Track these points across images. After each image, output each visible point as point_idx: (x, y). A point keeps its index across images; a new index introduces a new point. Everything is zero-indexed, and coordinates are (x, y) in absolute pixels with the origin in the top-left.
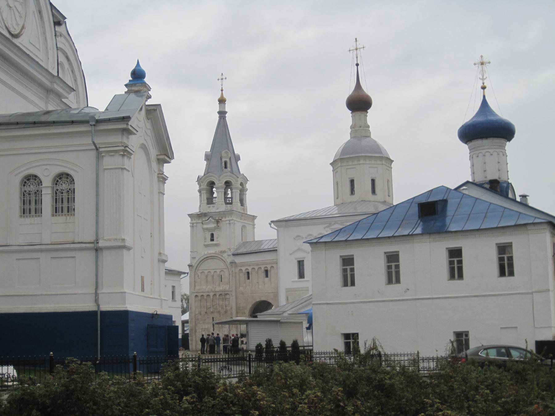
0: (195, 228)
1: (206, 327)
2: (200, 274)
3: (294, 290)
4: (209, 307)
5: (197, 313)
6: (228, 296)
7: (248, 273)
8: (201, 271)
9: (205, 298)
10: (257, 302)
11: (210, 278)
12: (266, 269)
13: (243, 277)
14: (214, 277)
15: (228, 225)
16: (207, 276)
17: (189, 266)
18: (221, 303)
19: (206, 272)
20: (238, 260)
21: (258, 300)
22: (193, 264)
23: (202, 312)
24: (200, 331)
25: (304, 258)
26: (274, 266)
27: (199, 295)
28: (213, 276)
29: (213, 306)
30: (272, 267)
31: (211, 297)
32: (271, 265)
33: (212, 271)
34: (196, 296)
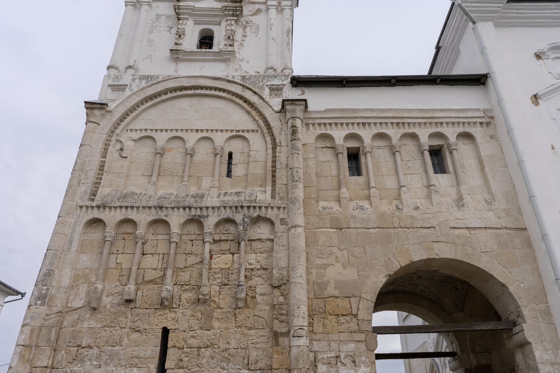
0: (145, 7)
2: (129, 144)
4: (150, 275)
5: (78, 303)
6: (263, 231)
8: (136, 136)
9: (141, 231)
10: (412, 263)
11: (175, 157)
12: (436, 142)
13: (334, 166)
14: (197, 158)
15: (273, 11)
16: (160, 153)
17: (90, 106)
18: (222, 261)
20: (319, 101)
22: (111, 106)
23: (106, 300)
26: (476, 131)
27: (111, 217)
28: (190, 154)
29: (177, 270)
30: (467, 136)
31: (175, 228)
32: (460, 129)
34: (96, 222)
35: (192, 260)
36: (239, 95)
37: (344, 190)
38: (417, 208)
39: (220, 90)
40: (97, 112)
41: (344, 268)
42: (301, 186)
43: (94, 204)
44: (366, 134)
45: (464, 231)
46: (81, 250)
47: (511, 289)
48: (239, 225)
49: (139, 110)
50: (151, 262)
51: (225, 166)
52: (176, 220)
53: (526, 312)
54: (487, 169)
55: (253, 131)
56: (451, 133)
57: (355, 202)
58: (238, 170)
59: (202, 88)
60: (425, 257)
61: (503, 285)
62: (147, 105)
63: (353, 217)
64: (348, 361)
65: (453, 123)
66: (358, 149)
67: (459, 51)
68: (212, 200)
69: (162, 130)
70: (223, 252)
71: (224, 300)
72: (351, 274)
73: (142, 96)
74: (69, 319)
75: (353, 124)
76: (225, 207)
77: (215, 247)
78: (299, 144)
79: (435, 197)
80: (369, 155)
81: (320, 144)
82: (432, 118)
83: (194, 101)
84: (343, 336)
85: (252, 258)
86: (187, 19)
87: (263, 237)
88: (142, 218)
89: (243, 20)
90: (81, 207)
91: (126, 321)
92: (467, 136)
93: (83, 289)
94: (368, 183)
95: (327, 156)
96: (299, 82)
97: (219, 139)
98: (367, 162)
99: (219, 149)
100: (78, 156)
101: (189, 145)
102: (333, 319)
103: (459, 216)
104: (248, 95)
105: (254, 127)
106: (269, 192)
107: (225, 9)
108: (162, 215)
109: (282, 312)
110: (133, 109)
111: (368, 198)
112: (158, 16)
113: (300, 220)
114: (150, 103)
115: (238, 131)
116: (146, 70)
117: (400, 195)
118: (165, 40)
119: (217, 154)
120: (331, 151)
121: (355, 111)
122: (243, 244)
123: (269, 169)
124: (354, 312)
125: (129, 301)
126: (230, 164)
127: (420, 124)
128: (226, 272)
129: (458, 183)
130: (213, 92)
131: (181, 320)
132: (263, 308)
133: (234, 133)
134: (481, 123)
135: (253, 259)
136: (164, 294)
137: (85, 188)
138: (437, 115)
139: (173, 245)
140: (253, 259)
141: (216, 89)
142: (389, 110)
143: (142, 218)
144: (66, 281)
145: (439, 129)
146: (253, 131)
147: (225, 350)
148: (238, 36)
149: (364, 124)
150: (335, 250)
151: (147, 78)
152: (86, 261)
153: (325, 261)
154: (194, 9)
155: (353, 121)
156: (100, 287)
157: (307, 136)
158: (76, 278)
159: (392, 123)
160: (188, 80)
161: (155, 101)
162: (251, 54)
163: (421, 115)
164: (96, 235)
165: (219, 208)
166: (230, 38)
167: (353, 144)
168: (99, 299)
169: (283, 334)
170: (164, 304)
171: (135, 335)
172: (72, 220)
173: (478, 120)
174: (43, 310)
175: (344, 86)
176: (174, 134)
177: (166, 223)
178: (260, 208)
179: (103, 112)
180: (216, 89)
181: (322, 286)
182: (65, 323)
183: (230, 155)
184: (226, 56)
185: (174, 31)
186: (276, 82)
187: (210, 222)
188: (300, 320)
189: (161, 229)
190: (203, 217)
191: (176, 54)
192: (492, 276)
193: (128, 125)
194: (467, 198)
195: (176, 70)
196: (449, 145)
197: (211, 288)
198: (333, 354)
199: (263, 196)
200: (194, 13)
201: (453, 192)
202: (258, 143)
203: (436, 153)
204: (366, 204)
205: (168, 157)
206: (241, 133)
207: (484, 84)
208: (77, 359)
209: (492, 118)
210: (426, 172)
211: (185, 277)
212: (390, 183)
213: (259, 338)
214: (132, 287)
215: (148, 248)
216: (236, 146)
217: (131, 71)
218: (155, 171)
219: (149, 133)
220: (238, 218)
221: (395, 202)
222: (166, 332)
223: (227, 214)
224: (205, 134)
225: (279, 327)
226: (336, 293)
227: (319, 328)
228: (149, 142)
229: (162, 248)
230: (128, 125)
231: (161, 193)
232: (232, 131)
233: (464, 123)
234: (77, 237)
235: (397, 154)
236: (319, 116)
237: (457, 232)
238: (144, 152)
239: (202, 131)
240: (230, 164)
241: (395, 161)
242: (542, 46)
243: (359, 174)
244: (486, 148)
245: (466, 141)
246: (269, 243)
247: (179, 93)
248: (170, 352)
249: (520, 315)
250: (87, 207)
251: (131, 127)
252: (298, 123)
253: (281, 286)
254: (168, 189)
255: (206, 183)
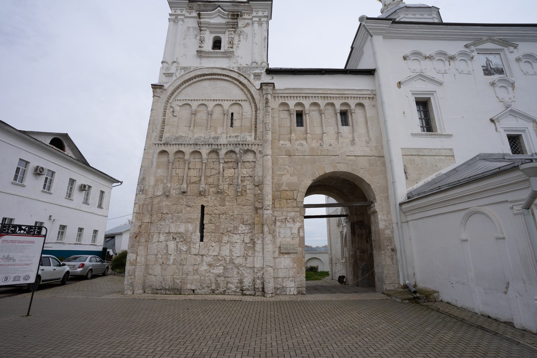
0: (180, 23)
1: (182, 229)
2: (177, 108)
3: (419, 153)
4: (193, 180)
5: (159, 193)
6: (250, 157)
7: (300, 115)
8: (180, 103)
9: (187, 157)
10: (326, 174)
11: (202, 116)
12: (344, 108)
13: (288, 121)
14: (214, 116)
15: (256, 25)
16: (194, 114)
17: (154, 86)
18: (229, 172)
19: (194, 105)
20: (282, 83)
21: (329, 170)
22: (166, 86)
23: (173, 192)
24: (162, 238)
25: (432, 93)
27: (171, 150)
28: (210, 114)
29: (207, 177)
30: (361, 105)
31: (204, 156)
32: (358, 101)
33: (211, 105)
34: (163, 152)
35: (214, 172)
36: (236, 78)
37: (293, 135)
38: (331, 145)
39: (226, 76)
40: (158, 90)
41: (291, 176)
42: (270, 133)
43: (162, 143)
44: (307, 103)
45: (354, 157)
46: (158, 167)
47: (372, 187)
48: (237, 154)
49: (181, 88)
50: (193, 173)
51: (230, 121)
52: (205, 151)
53: (377, 198)
54: (369, 124)
55: (245, 100)
56: (352, 103)
57: (299, 142)
58: (236, 123)
59: (215, 74)
60: (332, 171)
61: (369, 185)
62: (185, 85)
63: (297, 150)
64: (291, 220)
65: (354, 97)
66: (302, 111)
67: (363, 52)
68: (223, 140)
69: (194, 100)
70: (229, 168)
71: (231, 192)
72: (295, 179)
73: (182, 80)
74: (156, 201)
75: (300, 97)
76: (230, 144)
77: (225, 165)
78: (270, 109)
79: (341, 139)
80: (307, 115)
81: (282, 108)
82: (343, 94)
83: (212, 82)
84: (289, 209)
85: (244, 171)
86: (206, 30)
87: (250, 160)
88: (187, 150)
89: (238, 30)
90: (155, 144)
91: (184, 201)
92: (361, 105)
93: (161, 186)
94: (306, 131)
95: (285, 115)
96: (270, 72)
97: (226, 105)
98: (306, 119)
99: (226, 111)
100: (151, 116)
101: (210, 109)
102: (285, 201)
103: (351, 150)
104: (242, 79)
105: (245, 98)
106: (253, 136)
107: (228, 23)
108: (197, 148)
109: (259, 198)
110: (178, 88)
111: (306, 139)
112: (189, 28)
113: (269, 152)
114: (187, 84)
115: (236, 101)
116: (184, 63)
117: (322, 138)
118: (193, 45)
119: (225, 114)
120: (287, 112)
121: (301, 89)
122: (239, 164)
123: (253, 123)
124: (295, 197)
125: (184, 192)
126: (232, 119)
127: (336, 97)
128: (232, 178)
129: (353, 132)
130: (222, 77)
131: (210, 201)
132: (250, 196)
133: (234, 102)
134: (369, 98)
135: (245, 172)
136: (201, 189)
137: (156, 134)
138: (346, 92)
139: (204, 164)
140: (245, 172)
141: (223, 75)
142: (320, 89)
143: (187, 150)
144: (152, 183)
145: (346, 101)
146: (245, 100)
147: (232, 215)
148: (236, 42)
149: (306, 97)
150: (287, 167)
151: (184, 68)
152: (161, 172)
153: (282, 173)
154: (209, 24)
155: (300, 95)
156: (169, 185)
157: (274, 104)
158: (157, 181)
159: (321, 97)
160: (208, 69)
161: (190, 82)
162: (244, 53)
163: (337, 93)
164: (164, 159)
165: (227, 145)
166: (231, 43)
167: (299, 108)
168: (169, 191)
169: (260, 208)
170: (201, 194)
171: (188, 209)
172: (151, 151)
173: (368, 96)
174: (143, 196)
175: (296, 74)
176: (201, 102)
177: (200, 153)
178: (248, 145)
179: (162, 90)
180: (223, 75)
181: (280, 185)
182: (154, 203)
183: (232, 114)
184: (229, 55)
185: (198, 38)
186: (257, 71)
187: (223, 152)
188: (268, 201)
189: (197, 156)
190: (219, 149)
191: (200, 54)
192: (364, 180)
193: (175, 97)
194: (357, 140)
195: (201, 63)
196: (350, 110)
197: (224, 186)
198: (284, 217)
199: (250, 138)
200: (209, 26)
201: (350, 136)
202: (247, 108)
203: (344, 115)
204: (304, 142)
205: (199, 116)
206: (238, 102)
207: (373, 74)
208: (162, 219)
209: (375, 95)
210: (337, 125)
211: (211, 180)
212: (318, 131)
213: (248, 211)
214: (184, 185)
215: (191, 166)
216: (235, 109)
217: (175, 64)
218: (192, 124)
219: (187, 102)
220: (237, 150)
221: (320, 142)
222: (203, 207)
223: (231, 148)
224: (218, 102)
225: (258, 205)
226: (287, 188)
227: (277, 205)
228: (188, 107)
229: (198, 166)
230: (175, 97)
231: (196, 136)
232: (233, 100)
233: (360, 98)
234: (155, 160)
235: (323, 114)
236: (281, 92)
237: (350, 158)
238: (185, 113)
239: (216, 100)
240: (232, 119)
241: (321, 118)
242: (408, 52)
243: (302, 126)
244: (370, 112)
245: (360, 108)
246: (253, 163)
247: (203, 78)
248: (205, 216)
249: (375, 199)
250: (158, 144)
251: (177, 98)
252: (269, 97)
253: (259, 185)
254: (199, 134)
255: (219, 130)
